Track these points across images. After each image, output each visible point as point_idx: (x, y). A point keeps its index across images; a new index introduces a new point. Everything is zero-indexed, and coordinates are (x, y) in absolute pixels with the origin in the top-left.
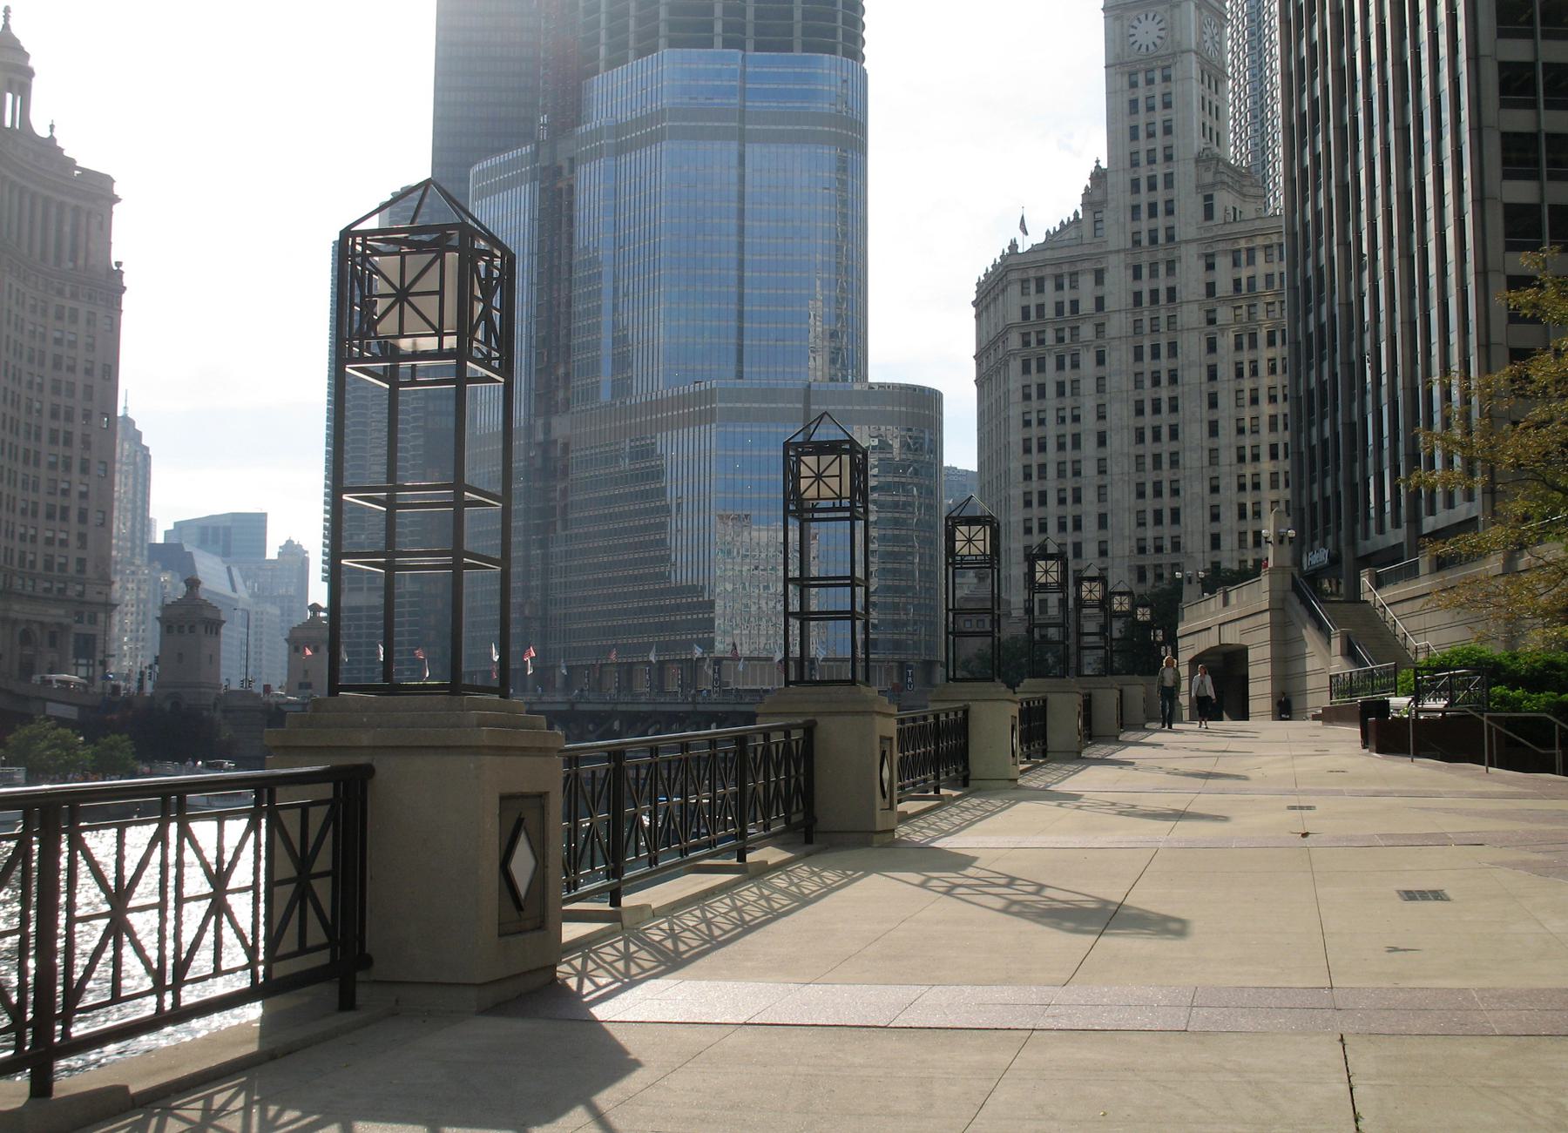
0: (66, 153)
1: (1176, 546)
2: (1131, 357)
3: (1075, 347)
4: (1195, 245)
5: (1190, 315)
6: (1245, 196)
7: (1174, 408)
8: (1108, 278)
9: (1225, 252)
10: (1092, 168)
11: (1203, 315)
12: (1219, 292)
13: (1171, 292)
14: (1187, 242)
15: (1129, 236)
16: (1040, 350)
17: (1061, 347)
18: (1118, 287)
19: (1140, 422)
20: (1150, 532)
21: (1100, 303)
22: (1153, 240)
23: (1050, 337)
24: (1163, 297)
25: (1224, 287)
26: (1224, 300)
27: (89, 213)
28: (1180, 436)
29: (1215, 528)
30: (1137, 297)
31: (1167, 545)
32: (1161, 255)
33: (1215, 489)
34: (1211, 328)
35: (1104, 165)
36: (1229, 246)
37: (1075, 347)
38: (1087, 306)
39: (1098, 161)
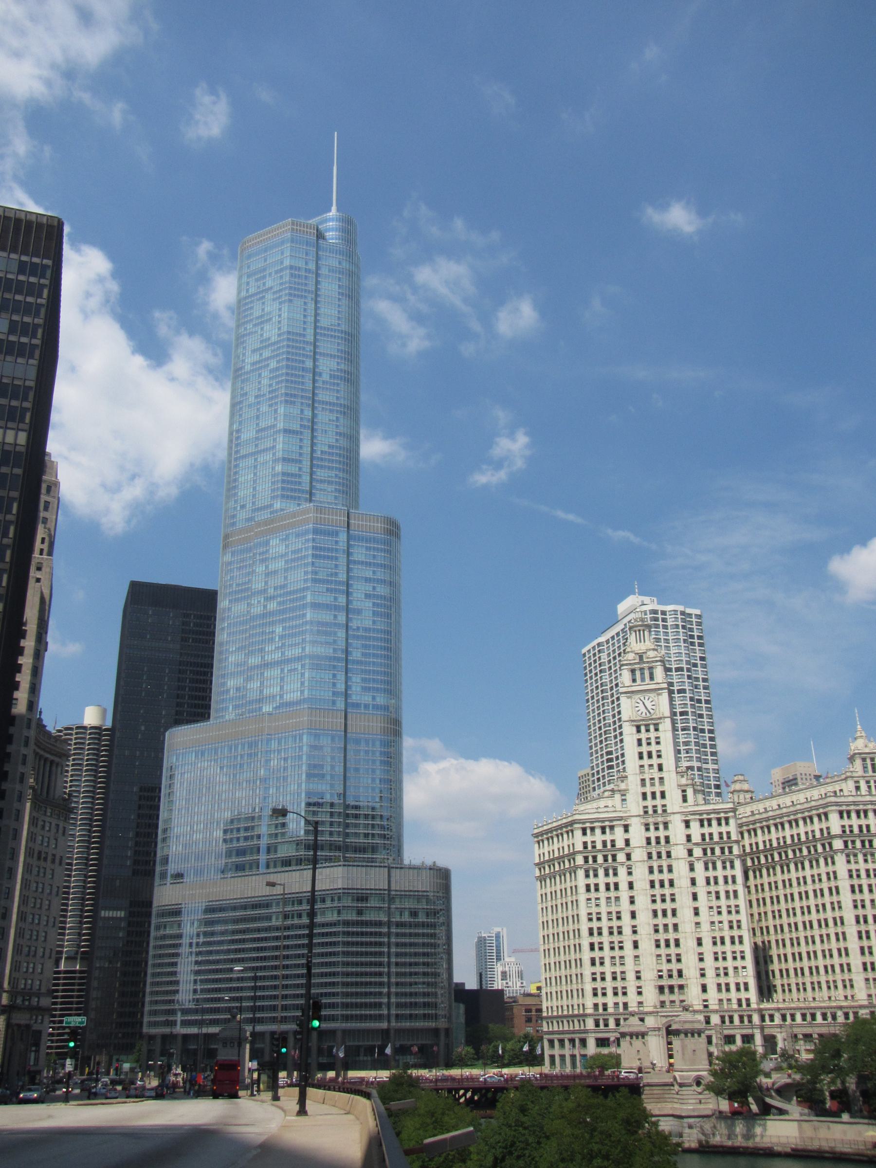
0: (47, 728)
1: (680, 973)
2: (647, 871)
3: (615, 865)
4: (679, 815)
5: (679, 851)
8: (630, 829)
11: (686, 852)
14: (674, 813)
15: (641, 808)
18: (637, 834)
19: (655, 907)
20: (665, 967)
21: (627, 842)
22: (655, 811)
23: (600, 859)
24: (663, 841)
25: (696, 838)
26: (697, 844)
27: (57, 764)
31: (675, 973)
32: (660, 819)
36: (698, 817)
37: (615, 865)
38: (620, 844)
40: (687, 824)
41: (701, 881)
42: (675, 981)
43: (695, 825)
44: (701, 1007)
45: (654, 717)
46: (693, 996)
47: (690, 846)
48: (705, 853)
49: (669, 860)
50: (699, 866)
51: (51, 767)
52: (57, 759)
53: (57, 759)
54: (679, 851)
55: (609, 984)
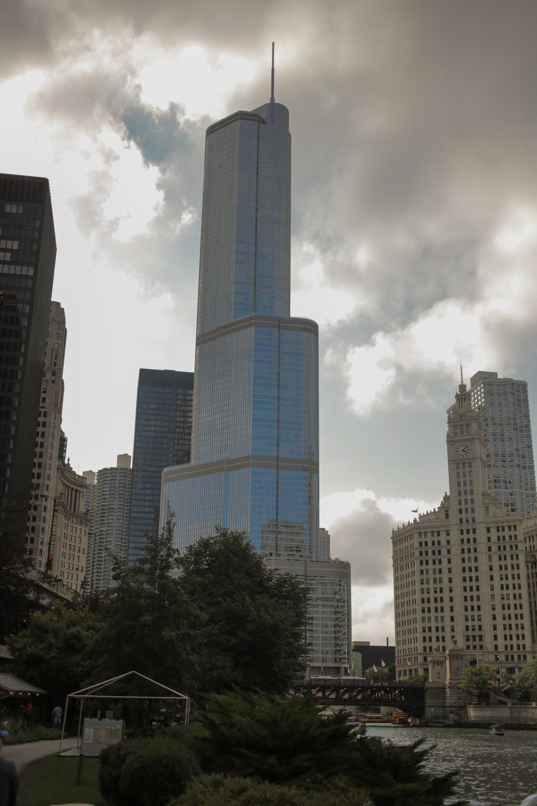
0: (73, 470)
1: (480, 628)
2: (461, 561)
3: (440, 557)
5: (482, 548)
6: (497, 507)
7: (477, 580)
8: (451, 533)
9: (494, 527)
10: (444, 495)
12: (492, 540)
13: (475, 540)
16: (427, 557)
17: (434, 557)
18: (455, 537)
21: (448, 542)
22: (467, 521)
25: (494, 539)
27: (80, 492)
28: (480, 590)
29: (495, 622)
30: (462, 541)
33: (494, 609)
34: (490, 553)
35: (448, 494)
36: (495, 525)
38: (444, 543)
39: (446, 493)
40: (488, 530)
41: (496, 568)
42: (477, 633)
43: (493, 530)
44: (493, 650)
45: (468, 458)
46: (488, 642)
47: (489, 544)
48: (500, 549)
49: (475, 554)
50: (495, 558)
51: (76, 493)
52: (79, 489)
53: (79, 489)
54: (482, 548)
55: (434, 634)
